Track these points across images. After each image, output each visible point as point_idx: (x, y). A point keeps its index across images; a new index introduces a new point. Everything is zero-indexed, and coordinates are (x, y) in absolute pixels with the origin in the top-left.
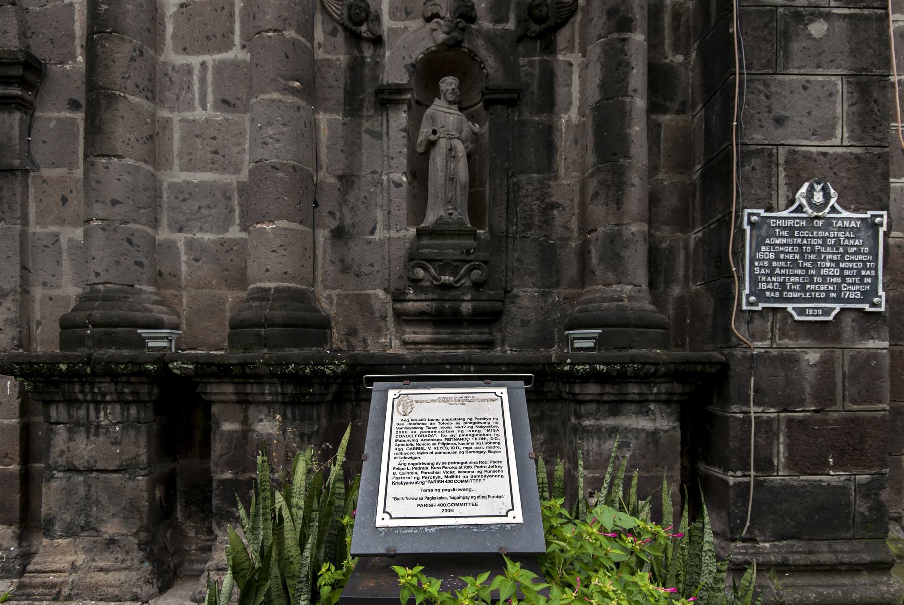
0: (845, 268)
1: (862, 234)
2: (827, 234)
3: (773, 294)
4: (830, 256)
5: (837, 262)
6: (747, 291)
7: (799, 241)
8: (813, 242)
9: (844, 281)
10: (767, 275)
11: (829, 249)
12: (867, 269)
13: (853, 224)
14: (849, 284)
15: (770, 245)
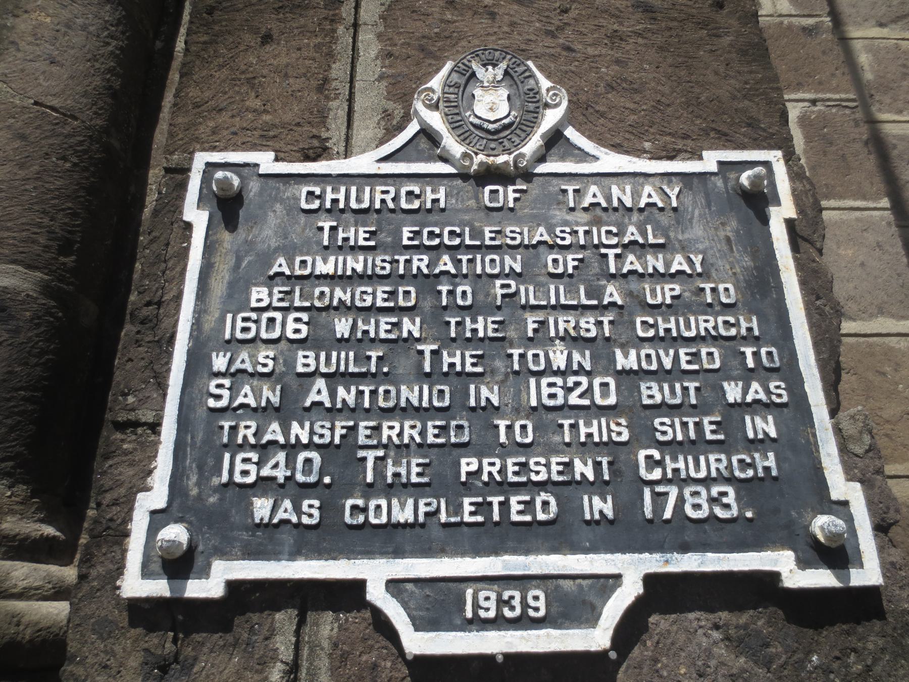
0: (641, 374)
1: (697, 231)
2: (541, 234)
3: (287, 510)
4: (564, 323)
5: (601, 349)
6: (156, 496)
7: (420, 262)
8: (484, 264)
9: (644, 434)
10: (264, 412)
11: (556, 293)
12: (748, 375)
13: (649, 194)
14: (672, 447)
15: (292, 279)
